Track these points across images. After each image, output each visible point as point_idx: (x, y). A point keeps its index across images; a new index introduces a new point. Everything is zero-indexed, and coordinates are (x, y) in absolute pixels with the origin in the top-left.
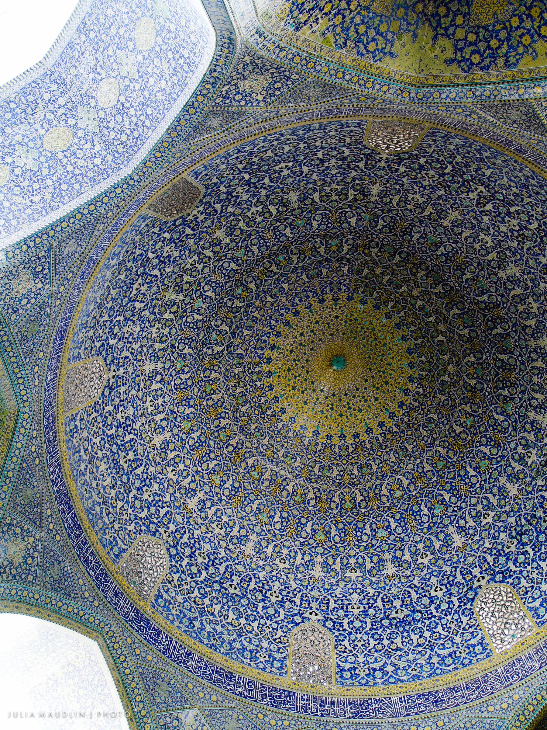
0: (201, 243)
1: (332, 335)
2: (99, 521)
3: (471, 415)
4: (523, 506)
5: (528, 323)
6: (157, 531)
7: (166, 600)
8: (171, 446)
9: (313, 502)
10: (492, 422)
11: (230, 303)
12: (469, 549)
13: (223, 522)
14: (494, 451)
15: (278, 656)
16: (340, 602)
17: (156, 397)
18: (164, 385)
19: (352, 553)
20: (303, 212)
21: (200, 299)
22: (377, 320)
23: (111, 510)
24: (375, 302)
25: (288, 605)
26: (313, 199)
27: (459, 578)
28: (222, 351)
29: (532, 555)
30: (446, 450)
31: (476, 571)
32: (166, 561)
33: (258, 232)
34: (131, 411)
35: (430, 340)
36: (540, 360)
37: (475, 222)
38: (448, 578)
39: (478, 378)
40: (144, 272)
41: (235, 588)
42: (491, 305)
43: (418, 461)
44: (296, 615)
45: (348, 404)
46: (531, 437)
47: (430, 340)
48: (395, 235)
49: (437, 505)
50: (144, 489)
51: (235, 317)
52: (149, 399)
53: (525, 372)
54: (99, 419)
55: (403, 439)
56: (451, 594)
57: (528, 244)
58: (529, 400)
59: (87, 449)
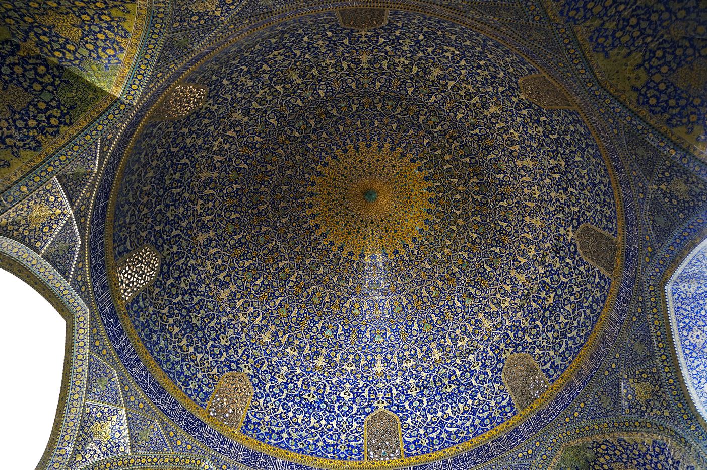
3: (439, 289)
4: (437, 370)
5: (519, 259)
14: (440, 322)
21: (311, 92)
22: (420, 186)
27: (366, 394)
28: (298, 138)
29: (425, 405)
30: (408, 301)
31: (380, 395)
35: (446, 224)
38: (358, 390)
40: (290, 48)
45: (359, 228)
46: (470, 329)
47: (446, 224)
56: (354, 402)
58: (485, 305)
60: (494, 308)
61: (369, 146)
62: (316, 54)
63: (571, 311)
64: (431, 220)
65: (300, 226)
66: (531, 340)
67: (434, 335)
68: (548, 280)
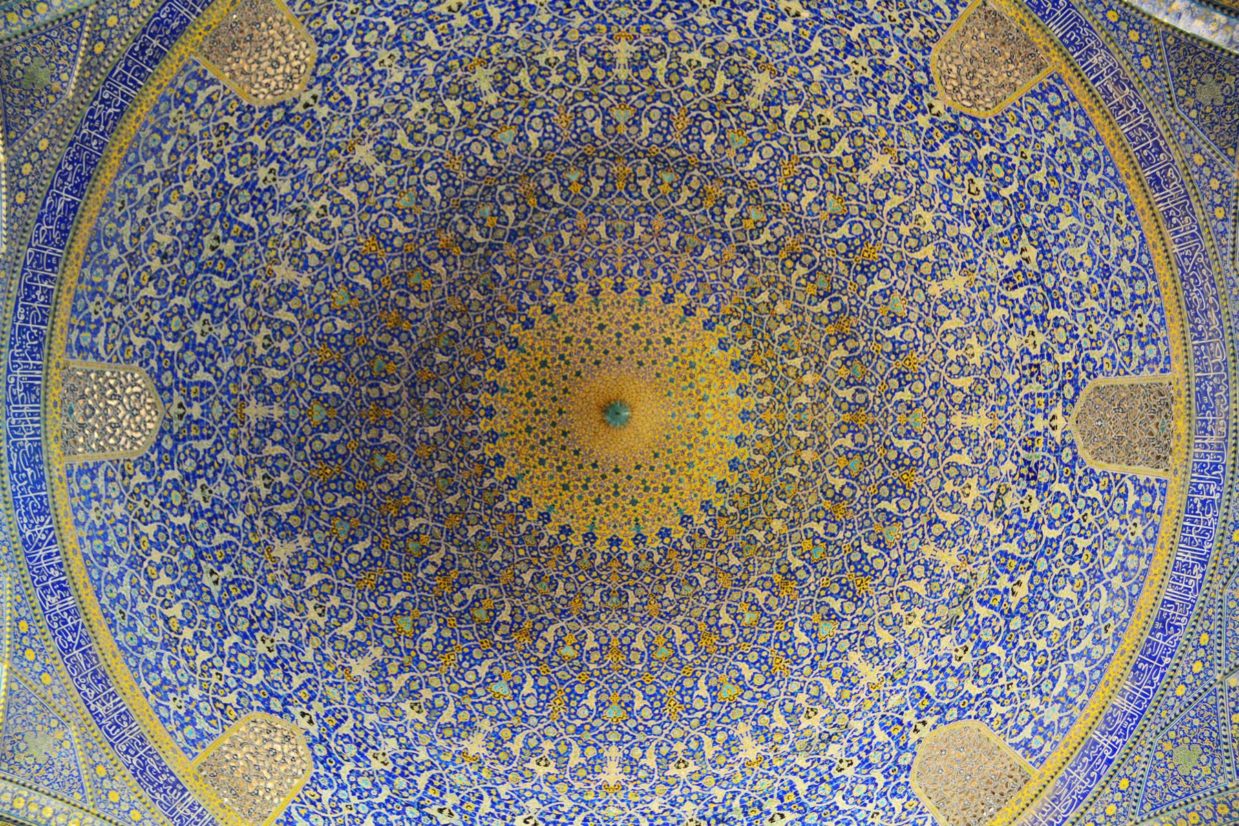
0: (588, 39)
1: (641, 364)
2: (99, 270)
3: (759, 609)
4: (750, 782)
5: (943, 516)
6: (170, 390)
7: (95, 488)
8: (295, 303)
9: (431, 570)
10: (784, 637)
11: (546, 182)
12: (621, 795)
13: (277, 480)
14: (759, 680)
15: (202, 724)
16: (361, 734)
17: (334, 209)
18: (361, 206)
19: (435, 682)
20: (755, 123)
23: (131, 282)
24: (739, 356)
25: (276, 674)
26: (784, 112)
28: (478, 245)
30: (686, 636)
32: (144, 442)
33: (671, 102)
34: (284, 187)
35: (777, 465)
36: (924, 581)
37: (979, 310)
38: (558, 817)
39: (809, 561)
41: (216, 582)
42: (907, 461)
43: (632, 626)
44: (278, 697)
47: (777, 465)
48: (849, 264)
49: (615, 705)
50: (205, 316)
51: (536, 211)
52: (324, 200)
53: (887, 590)
54: (233, 137)
55: (631, 582)
57: (1035, 387)
58: (866, 633)
59: (178, 155)
60: (886, 637)
61: (619, 288)
62: (530, 28)
63: (1074, 597)
64: (744, 460)
65: (464, 452)
66: (979, 691)
67: (744, 708)
68: (1013, 548)
